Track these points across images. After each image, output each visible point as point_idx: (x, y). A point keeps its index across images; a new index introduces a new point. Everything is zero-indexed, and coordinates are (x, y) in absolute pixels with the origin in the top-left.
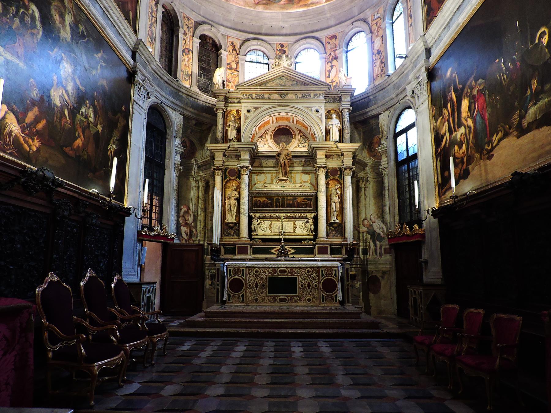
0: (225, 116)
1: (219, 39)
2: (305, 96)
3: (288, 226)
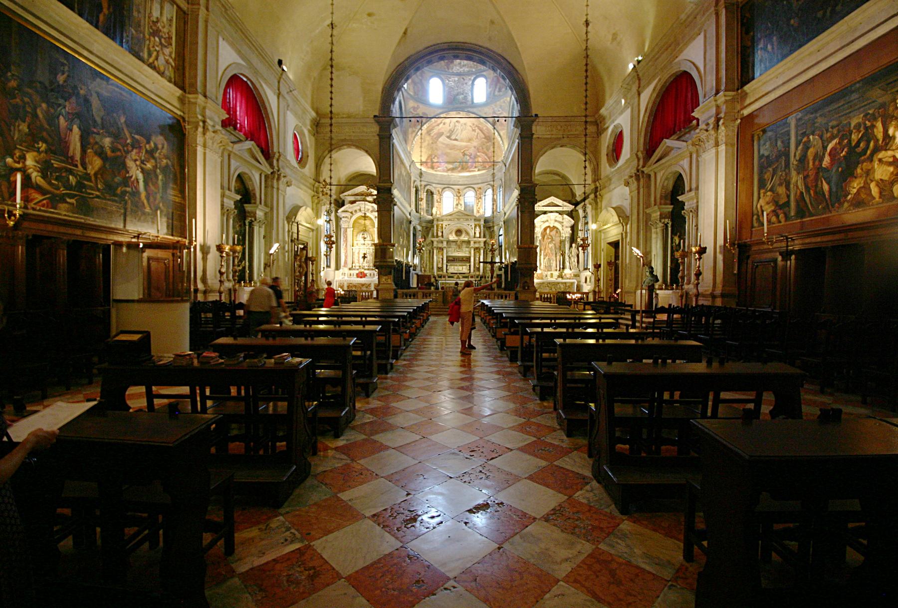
0: (437, 226)
1: (433, 190)
2: (467, 220)
3: (460, 268)
